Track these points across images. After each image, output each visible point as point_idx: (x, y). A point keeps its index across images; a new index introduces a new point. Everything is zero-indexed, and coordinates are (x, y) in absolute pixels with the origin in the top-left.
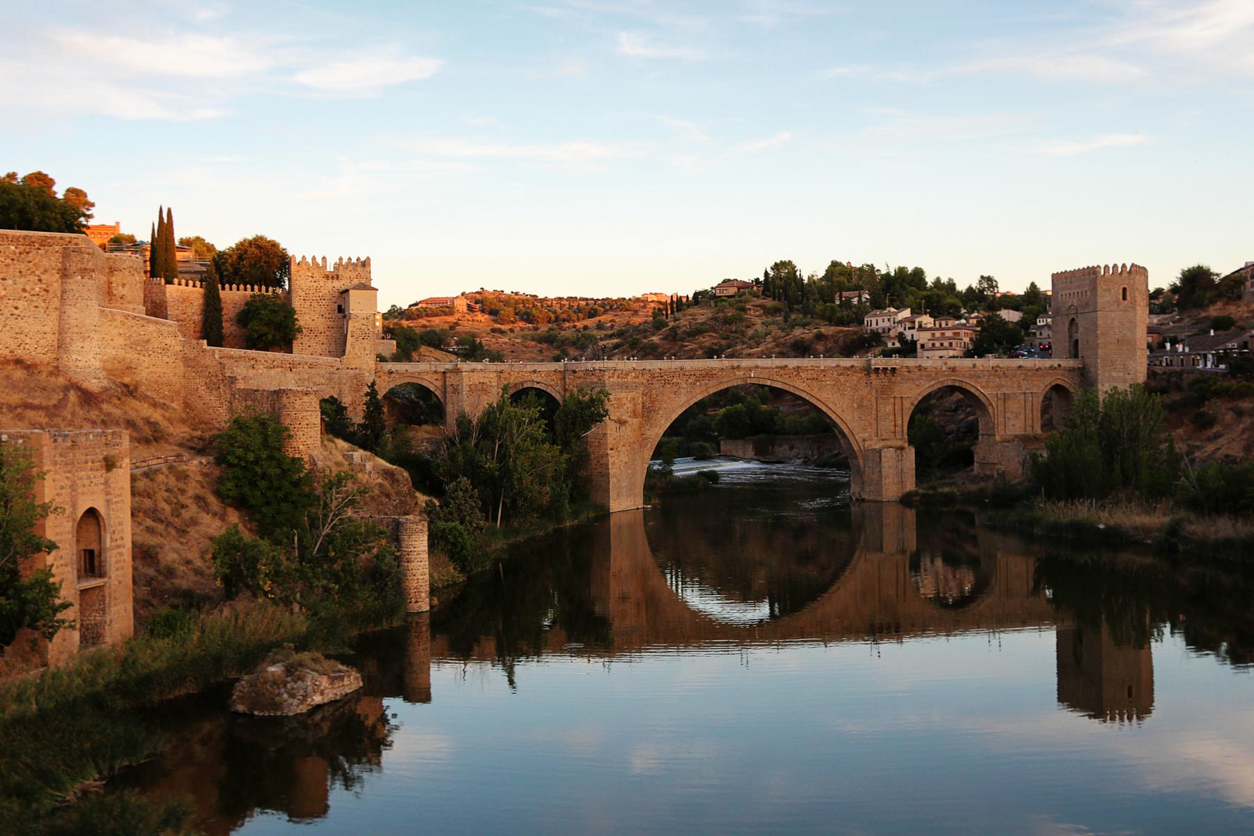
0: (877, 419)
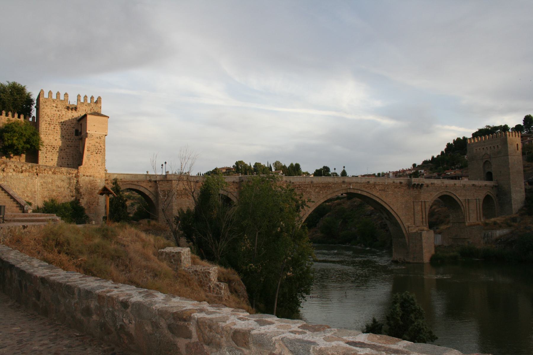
0: (414, 214)
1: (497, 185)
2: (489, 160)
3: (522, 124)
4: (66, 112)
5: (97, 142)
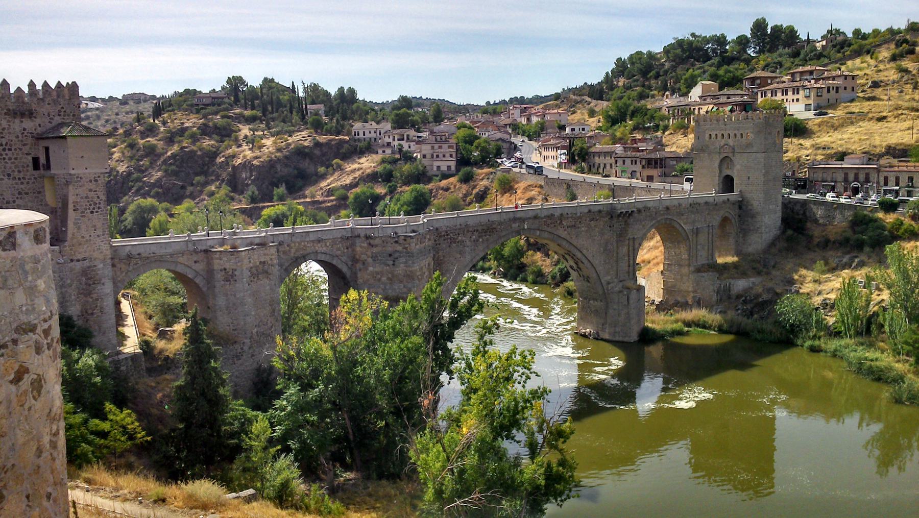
0: (617, 261)
1: (741, 199)
2: (730, 155)
3: (749, 36)
4: (9, 121)
5: (91, 190)
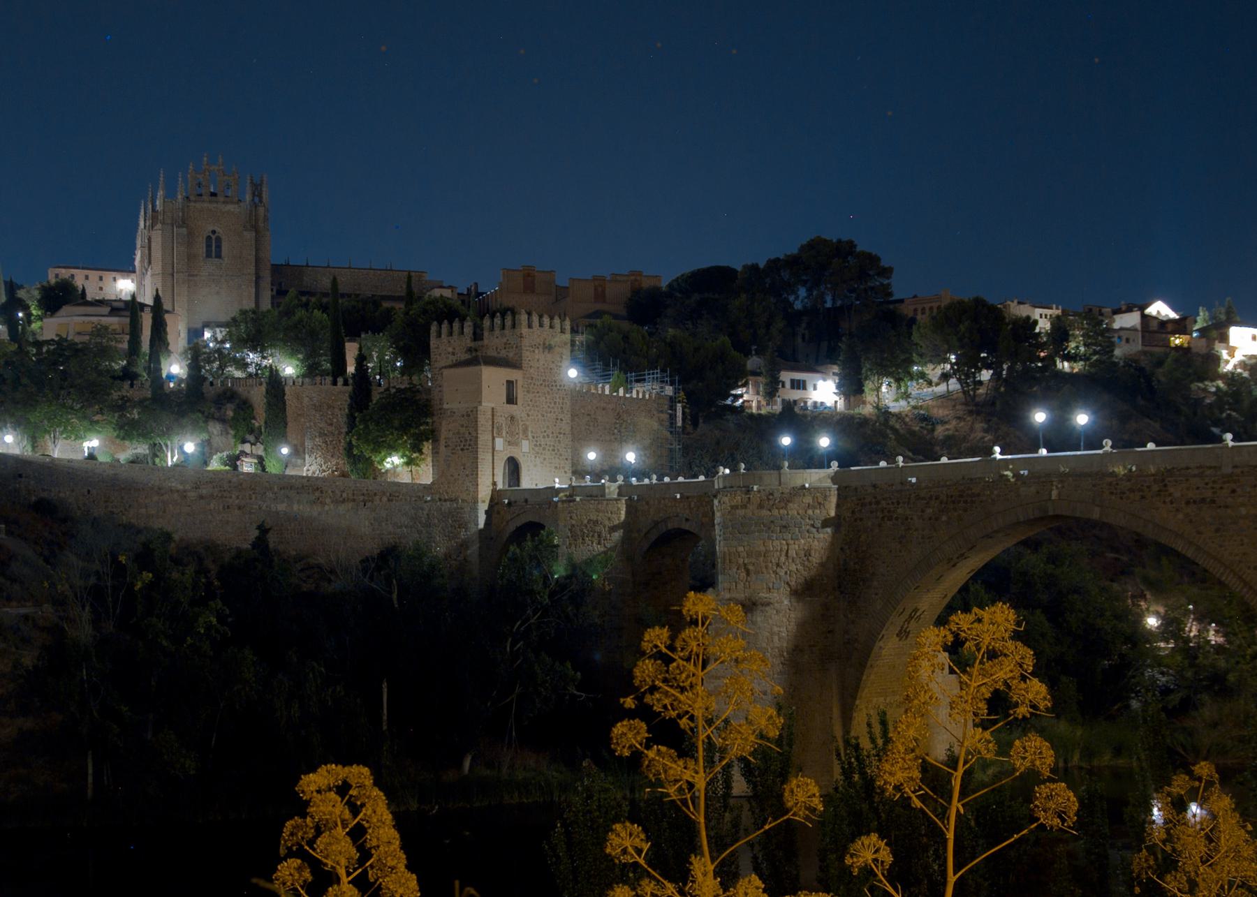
5: (462, 426)
